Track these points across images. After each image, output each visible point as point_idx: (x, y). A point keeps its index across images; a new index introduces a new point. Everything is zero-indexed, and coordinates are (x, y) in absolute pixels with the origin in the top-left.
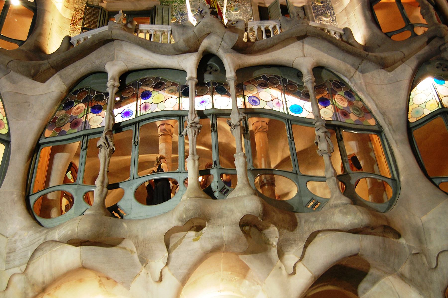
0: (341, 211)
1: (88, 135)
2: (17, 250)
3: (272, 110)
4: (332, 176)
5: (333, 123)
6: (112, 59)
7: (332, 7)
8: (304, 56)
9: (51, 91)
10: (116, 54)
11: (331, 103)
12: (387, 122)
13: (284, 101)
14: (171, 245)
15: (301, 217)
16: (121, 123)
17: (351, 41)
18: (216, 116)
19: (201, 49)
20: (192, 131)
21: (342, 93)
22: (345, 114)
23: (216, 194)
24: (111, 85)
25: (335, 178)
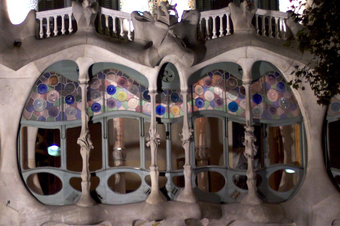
0: (252, 211)
2: (27, 221)
3: (214, 110)
6: (82, 56)
8: (247, 57)
9: (27, 77)
10: (85, 50)
12: (308, 116)
13: (224, 98)
18: (171, 124)
19: (162, 63)
20: (154, 145)
22: (273, 110)
23: (169, 194)
24: (83, 79)
25: (253, 181)
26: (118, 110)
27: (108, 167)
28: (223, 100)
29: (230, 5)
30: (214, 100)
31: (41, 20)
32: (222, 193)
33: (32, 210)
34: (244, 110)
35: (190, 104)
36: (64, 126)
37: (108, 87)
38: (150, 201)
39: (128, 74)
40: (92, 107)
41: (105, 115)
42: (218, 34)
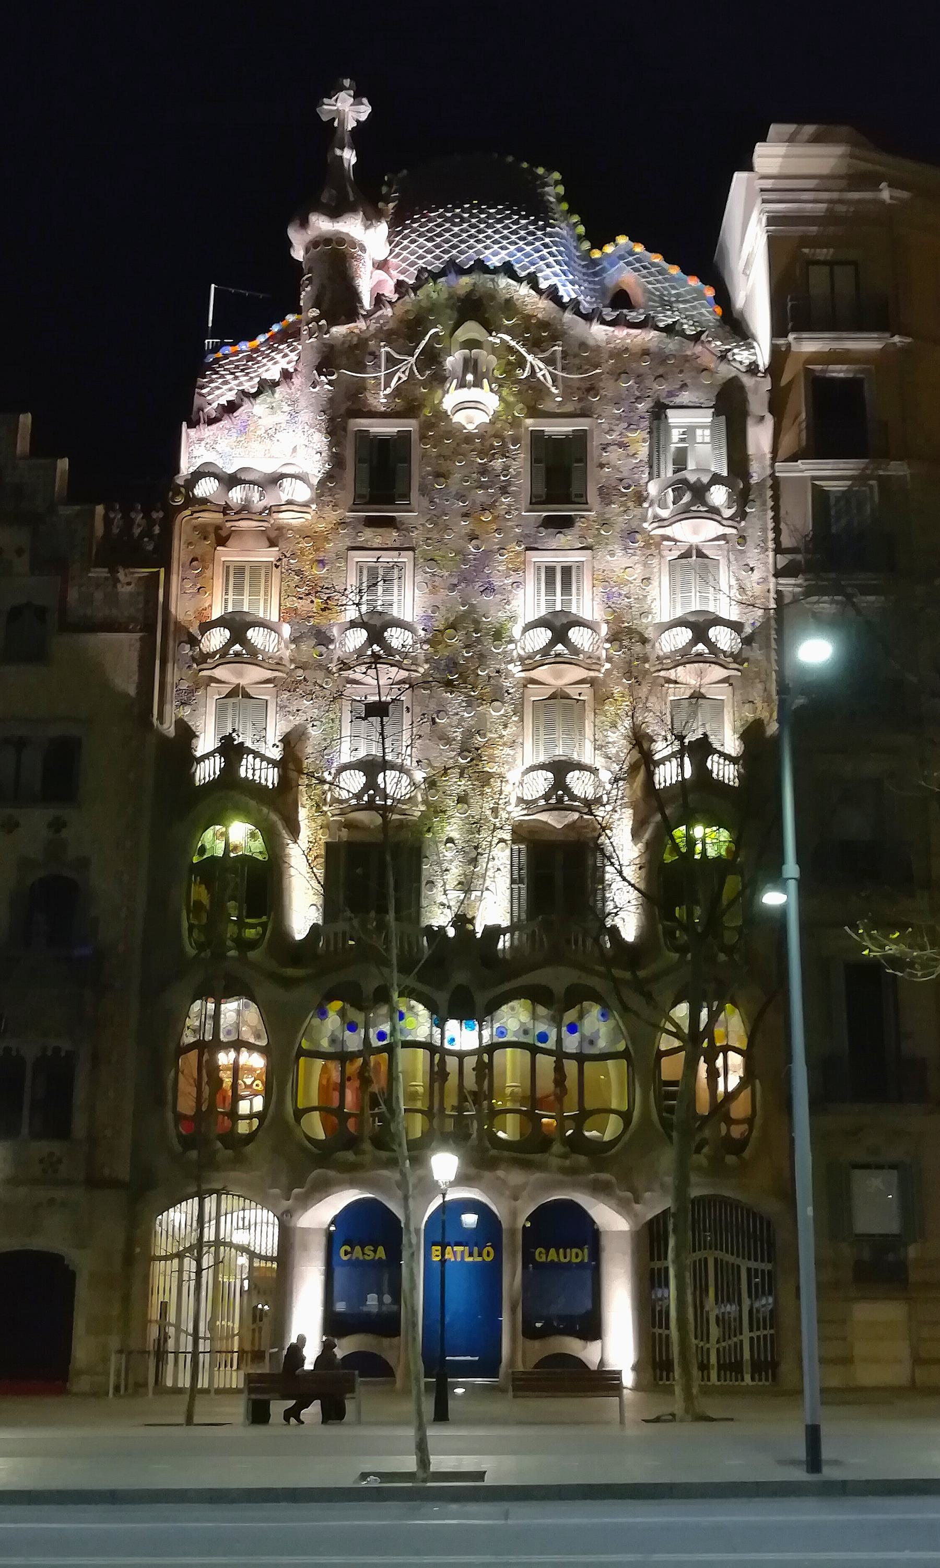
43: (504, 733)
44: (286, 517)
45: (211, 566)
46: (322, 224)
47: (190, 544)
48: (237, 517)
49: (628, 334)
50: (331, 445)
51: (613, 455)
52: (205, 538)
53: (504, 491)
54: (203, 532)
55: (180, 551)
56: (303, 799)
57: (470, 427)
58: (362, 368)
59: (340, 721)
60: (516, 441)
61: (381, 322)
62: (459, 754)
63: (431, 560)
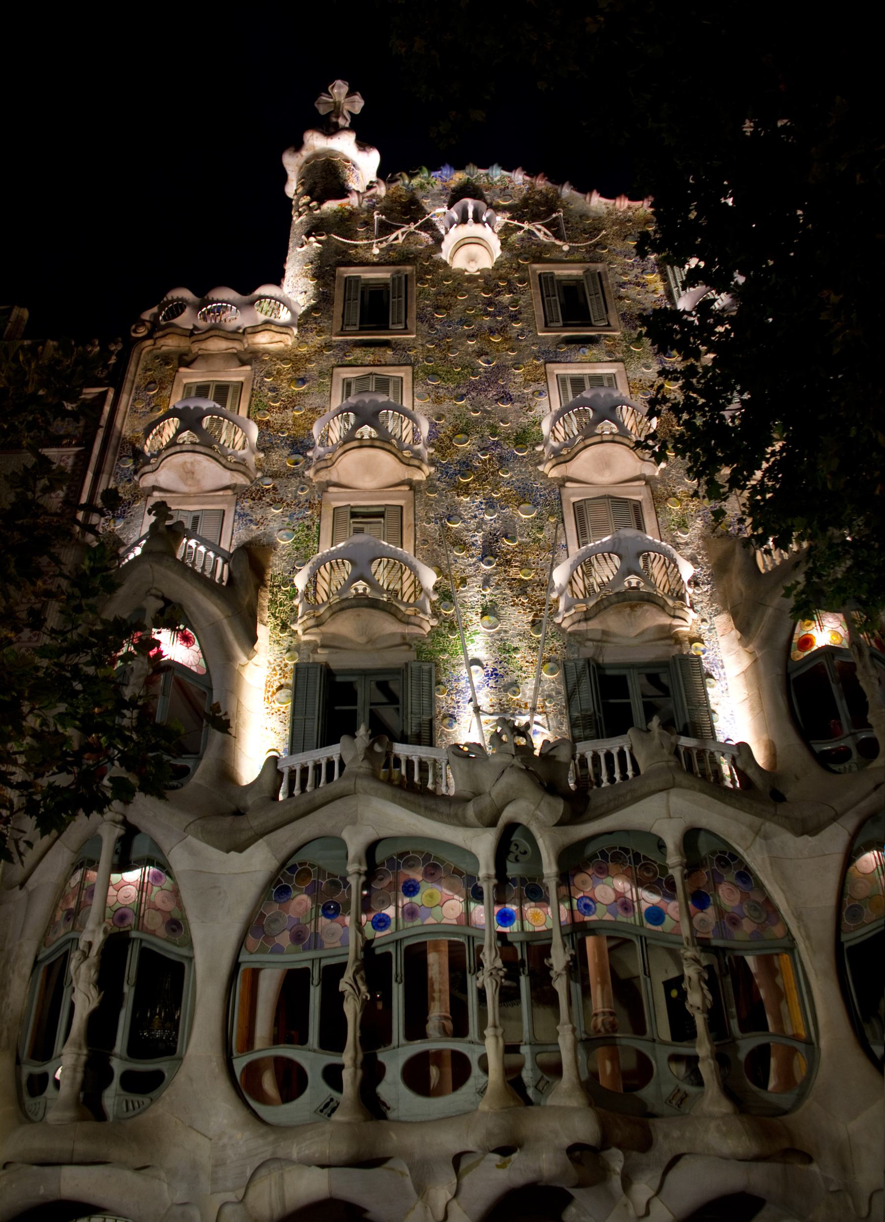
1: (320, 959)
2: (228, 1161)
4: (707, 1057)
5: (714, 943)
6: (354, 821)
7: (722, 661)
8: (670, 817)
11: (712, 901)
12: (804, 934)
13: (635, 899)
14: (461, 1170)
15: (659, 1127)
16: (372, 941)
17: (750, 772)
18: (527, 943)
19: (501, 822)
20: (492, 982)
21: (730, 876)
22: (735, 922)
23: (530, 1092)
24: (354, 868)
25: (711, 1062)
26: (423, 925)
27: (402, 1041)
28: (633, 901)
29: (630, 732)
30: (615, 901)
31: (286, 771)
32: (647, 1093)
33: (239, 1136)
34: (678, 922)
35: (564, 908)
36: (318, 961)
37: (405, 883)
38: (484, 1106)
39: (443, 855)
40: (372, 922)
41: (398, 936)
42: (611, 779)
43: (541, 536)
44: (264, 340)
45: (170, 387)
46: (316, 142)
47: (150, 370)
48: (204, 336)
49: (629, 208)
50: (317, 287)
51: (632, 291)
52: (167, 364)
53: (515, 318)
54: (166, 359)
55: (135, 373)
56: (266, 615)
57: (472, 269)
58: (350, 234)
59: (319, 528)
60: (521, 281)
61: (374, 200)
62: (481, 560)
63: (433, 374)
